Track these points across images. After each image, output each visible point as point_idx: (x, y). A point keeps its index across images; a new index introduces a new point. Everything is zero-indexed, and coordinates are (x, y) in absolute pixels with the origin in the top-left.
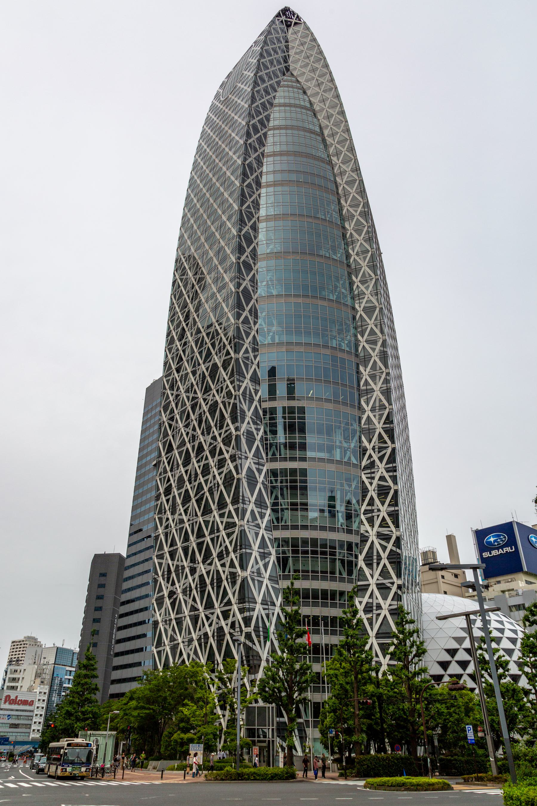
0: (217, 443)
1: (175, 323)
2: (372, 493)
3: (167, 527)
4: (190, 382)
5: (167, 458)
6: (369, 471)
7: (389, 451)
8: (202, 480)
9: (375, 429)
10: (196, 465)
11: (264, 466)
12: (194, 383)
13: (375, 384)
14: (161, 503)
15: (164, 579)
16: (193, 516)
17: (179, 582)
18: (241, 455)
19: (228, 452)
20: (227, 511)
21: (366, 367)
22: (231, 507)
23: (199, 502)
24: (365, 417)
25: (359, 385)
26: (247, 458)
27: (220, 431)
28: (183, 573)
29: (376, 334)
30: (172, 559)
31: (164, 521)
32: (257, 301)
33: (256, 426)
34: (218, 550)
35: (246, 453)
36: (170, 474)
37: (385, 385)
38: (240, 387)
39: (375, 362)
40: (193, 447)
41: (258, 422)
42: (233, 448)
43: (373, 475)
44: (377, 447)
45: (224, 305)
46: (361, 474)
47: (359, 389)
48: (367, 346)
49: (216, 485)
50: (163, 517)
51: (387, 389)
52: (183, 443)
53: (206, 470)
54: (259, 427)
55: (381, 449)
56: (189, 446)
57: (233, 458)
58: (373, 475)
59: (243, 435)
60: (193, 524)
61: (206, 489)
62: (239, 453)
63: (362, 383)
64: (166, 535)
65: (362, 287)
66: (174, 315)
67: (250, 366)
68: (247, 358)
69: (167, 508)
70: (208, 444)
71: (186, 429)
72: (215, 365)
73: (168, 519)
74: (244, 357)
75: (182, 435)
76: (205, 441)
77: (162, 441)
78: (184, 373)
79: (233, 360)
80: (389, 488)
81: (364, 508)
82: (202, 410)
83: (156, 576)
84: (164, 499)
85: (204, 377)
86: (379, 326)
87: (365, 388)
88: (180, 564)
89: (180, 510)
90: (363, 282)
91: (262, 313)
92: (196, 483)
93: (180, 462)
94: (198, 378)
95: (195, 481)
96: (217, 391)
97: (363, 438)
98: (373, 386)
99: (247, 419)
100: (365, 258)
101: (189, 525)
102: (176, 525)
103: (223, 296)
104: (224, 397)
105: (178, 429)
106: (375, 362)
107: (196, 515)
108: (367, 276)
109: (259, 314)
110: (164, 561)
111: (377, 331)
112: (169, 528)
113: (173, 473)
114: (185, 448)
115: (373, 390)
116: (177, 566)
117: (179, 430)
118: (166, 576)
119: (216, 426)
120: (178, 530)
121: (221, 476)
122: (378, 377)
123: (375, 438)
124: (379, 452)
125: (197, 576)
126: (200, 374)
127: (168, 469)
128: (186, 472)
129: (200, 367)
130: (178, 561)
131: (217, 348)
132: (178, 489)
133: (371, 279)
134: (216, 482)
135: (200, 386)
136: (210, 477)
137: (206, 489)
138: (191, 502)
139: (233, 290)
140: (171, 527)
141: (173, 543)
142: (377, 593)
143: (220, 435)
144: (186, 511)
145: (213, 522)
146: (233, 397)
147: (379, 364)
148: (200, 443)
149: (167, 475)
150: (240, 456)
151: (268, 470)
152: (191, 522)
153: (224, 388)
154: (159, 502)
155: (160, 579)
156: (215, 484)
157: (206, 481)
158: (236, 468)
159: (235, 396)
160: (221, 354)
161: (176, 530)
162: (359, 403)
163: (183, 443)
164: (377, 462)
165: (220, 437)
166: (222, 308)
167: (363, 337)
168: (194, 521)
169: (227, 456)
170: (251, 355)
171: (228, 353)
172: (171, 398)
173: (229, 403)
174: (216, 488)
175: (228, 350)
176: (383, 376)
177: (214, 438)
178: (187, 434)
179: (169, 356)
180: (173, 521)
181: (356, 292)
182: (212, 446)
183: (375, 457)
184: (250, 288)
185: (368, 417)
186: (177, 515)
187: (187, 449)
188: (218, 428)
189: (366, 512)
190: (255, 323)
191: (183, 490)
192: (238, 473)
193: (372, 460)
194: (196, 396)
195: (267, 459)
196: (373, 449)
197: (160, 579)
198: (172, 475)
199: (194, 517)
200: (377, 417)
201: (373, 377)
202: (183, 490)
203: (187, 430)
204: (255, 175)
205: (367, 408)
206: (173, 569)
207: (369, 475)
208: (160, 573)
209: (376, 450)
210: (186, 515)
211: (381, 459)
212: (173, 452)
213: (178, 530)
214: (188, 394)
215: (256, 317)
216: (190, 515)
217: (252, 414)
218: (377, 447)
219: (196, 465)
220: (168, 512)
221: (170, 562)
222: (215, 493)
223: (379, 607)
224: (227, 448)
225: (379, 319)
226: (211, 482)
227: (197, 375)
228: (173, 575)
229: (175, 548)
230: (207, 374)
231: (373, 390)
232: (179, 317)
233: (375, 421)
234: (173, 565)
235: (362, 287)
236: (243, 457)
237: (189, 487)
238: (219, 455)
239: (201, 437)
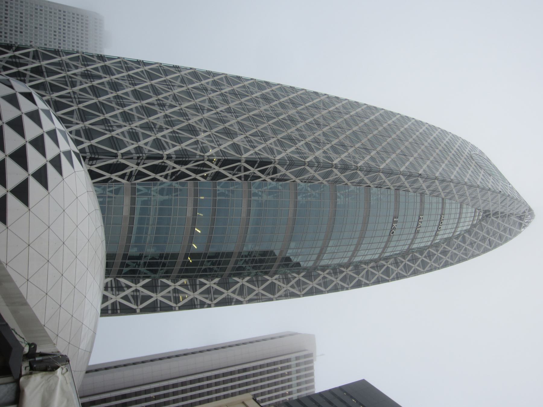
0: (156, 133)
1: (278, 93)
3: (68, 65)
4: (219, 105)
5: (142, 72)
6: (114, 285)
7: (134, 306)
8: (117, 112)
9: (156, 292)
10: (133, 106)
11: (128, 180)
12: (218, 110)
13: (201, 293)
15: (11, 57)
16: (79, 98)
18: (141, 160)
19: (146, 144)
20: (83, 139)
21: (218, 284)
23: (94, 106)
25: (201, 277)
26: (138, 164)
27: (167, 137)
29: (248, 295)
30: (33, 70)
31: (75, 63)
32: (294, 181)
33: (170, 175)
35: (144, 164)
36: (125, 74)
37: (199, 303)
38: (211, 161)
39: (222, 293)
40: (152, 104)
41: (174, 177)
42: (149, 151)
43: (109, 289)
44: (138, 294)
45: (293, 149)
46: (111, 277)
47: (196, 277)
48: (238, 286)
49: (111, 128)
50: (79, 62)
51: (195, 305)
52: (156, 92)
53: (127, 117)
54: (169, 177)
55: (135, 298)
57: (139, 150)
58: (109, 289)
59: (162, 162)
60: (70, 97)
61: (107, 116)
62: (144, 158)
63: (203, 280)
64: (59, 64)
66: (286, 92)
67: (231, 172)
68: (239, 170)
69: (89, 68)
70: (155, 122)
71: (171, 97)
72: (235, 135)
73: (77, 67)
74: (241, 167)
76: (158, 118)
77: (160, 68)
78: (229, 98)
79: (240, 156)
82: (190, 116)
83: (14, 48)
84: (99, 65)
85: (224, 122)
86: (256, 297)
87: (198, 283)
88: (27, 79)
89: (87, 83)
90: (298, 283)
91: (281, 185)
92: (114, 105)
93: (137, 87)
95: (117, 104)
97: (147, 280)
99: (178, 167)
100: (320, 284)
101: (69, 93)
102: (71, 77)
103: (302, 148)
104: (202, 143)
105: (172, 88)
106: (222, 293)
107: (80, 103)
108: (304, 287)
109: (281, 183)
110: (30, 59)
111: (251, 296)
112: (66, 69)
113: (126, 78)
114: (151, 94)
115: (194, 290)
116: (24, 75)
118: (14, 60)
120: (64, 79)
121: (120, 134)
122: (207, 296)
124: (133, 296)
126: (226, 117)
127: (131, 73)
128: (126, 94)
129: (234, 118)
130: (31, 76)
131: (252, 138)
132: (109, 83)
133: (300, 291)
134: (115, 128)
135: (215, 116)
136: (121, 122)
137: (107, 116)
138: (94, 98)
139: (307, 160)
140: (69, 71)
141: (51, 73)
143: (164, 136)
144: (84, 90)
146: (202, 154)
147: (220, 298)
148: (156, 113)
149: (125, 71)
150: (141, 158)
151: (123, 184)
152: (73, 96)
154: (95, 59)
155: (11, 53)
156: (112, 126)
157: (115, 116)
158: (129, 153)
159: (203, 156)
160: (246, 143)
161: (64, 77)
162: (183, 277)
163: (156, 92)
164: (123, 294)
165: (162, 136)
166: (291, 147)
167: (247, 282)
168: (74, 100)
169: (141, 143)
170: (242, 174)
172: (204, 82)
174: (107, 128)
175: (249, 150)
176: (208, 302)
177: (161, 129)
178: (166, 98)
179: (246, 83)
180: (75, 74)
181: (290, 276)
182: (153, 127)
183: (128, 292)
184: (306, 176)
185: (169, 286)
186: (81, 79)
187: (151, 97)
188: (171, 134)
190: (272, 179)
191: (107, 89)
192: (123, 155)
193: (125, 289)
194: (205, 111)
195: (135, 184)
196: (137, 290)
197: (11, 53)
198: (124, 77)
199: (77, 100)
200: (169, 295)
202: (107, 89)
204: (407, 185)
205: (177, 285)
206: (21, 69)
207: (109, 285)
208: (17, 53)
209: (135, 294)
210: (81, 90)
211: (126, 298)
212: (148, 81)
213: (64, 79)
214: (207, 101)
215: (279, 180)
216: (80, 95)
217: (183, 172)
218: (138, 294)
219: (133, 106)
220: (84, 69)
224: (150, 144)
225: (263, 297)
226: (114, 122)
227: (226, 114)
228: (15, 70)
229: (45, 74)
231: (194, 290)
232: (284, 97)
233: (164, 293)
234: (26, 70)
235: (293, 282)
236: (139, 161)
237: (110, 96)
238: (143, 133)
239: (163, 114)
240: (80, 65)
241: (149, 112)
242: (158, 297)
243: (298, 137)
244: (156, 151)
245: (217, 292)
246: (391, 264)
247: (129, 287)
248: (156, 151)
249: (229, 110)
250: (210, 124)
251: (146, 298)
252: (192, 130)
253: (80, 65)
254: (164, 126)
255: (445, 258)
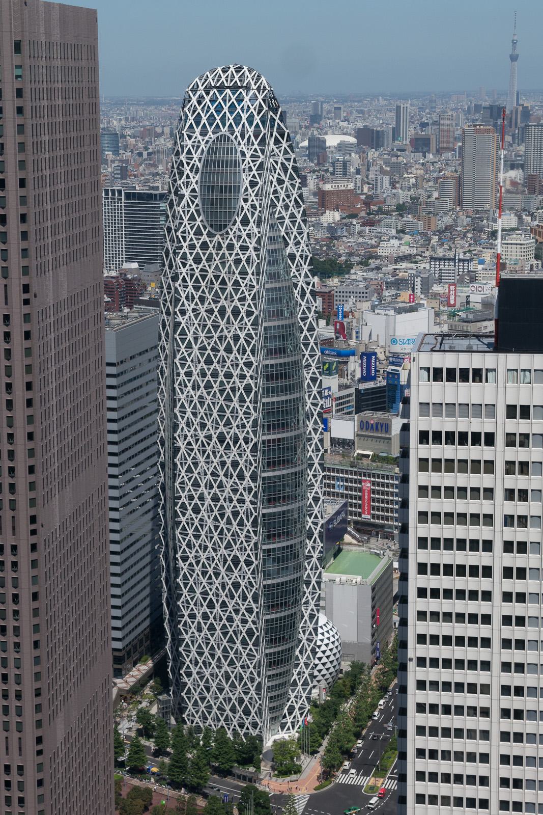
2: (306, 617)
7: (317, 594)
14: (185, 621)
17: (206, 668)
22: (251, 646)
23: (225, 634)
24: (307, 573)
28: (210, 666)
34: (240, 664)
40: (217, 601)
52: (205, 593)
55: (313, 593)
56: (211, 596)
64: (192, 642)
65: (313, 480)
75: (204, 587)
80: (315, 615)
81: (302, 625)
85: (225, 561)
94: (219, 556)
96: (240, 576)
98: (313, 554)
107: (222, 640)
110: (191, 655)
111: (319, 516)
117: (202, 583)
119: (239, 597)
123: (311, 586)
125: (223, 670)
142: (304, 666)
144: (212, 635)
145: (237, 649)
147: (318, 540)
153: (247, 578)
160: (243, 553)
164: (311, 600)
169: (250, 620)
171: (249, 556)
173: (251, 590)
176: (319, 548)
180: (200, 636)
187: (211, 599)
189: (302, 627)
201: (313, 548)
203: (211, 587)
205: (309, 568)
206: (201, 662)
211: (313, 599)
221: (198, 658)
222: (239, 635)
223: (304, 673)
230: (229, 559)
235: (313, 480)
240: (191, 631)
241: (224, 605)
242: (314, 580)
243: (233, 505)
244: (254, 614)
245: (315, 542)
246: (308, 373)
247: (307, 597)
248: (254, 614)
249: (215, 550)
250: (229, 569)
251: (314, 588)
252: (236, 585)
253: (191, 631)
254: (234, 601)
255: (308, 295)
